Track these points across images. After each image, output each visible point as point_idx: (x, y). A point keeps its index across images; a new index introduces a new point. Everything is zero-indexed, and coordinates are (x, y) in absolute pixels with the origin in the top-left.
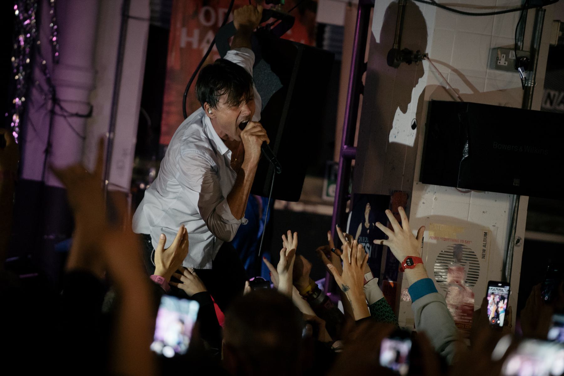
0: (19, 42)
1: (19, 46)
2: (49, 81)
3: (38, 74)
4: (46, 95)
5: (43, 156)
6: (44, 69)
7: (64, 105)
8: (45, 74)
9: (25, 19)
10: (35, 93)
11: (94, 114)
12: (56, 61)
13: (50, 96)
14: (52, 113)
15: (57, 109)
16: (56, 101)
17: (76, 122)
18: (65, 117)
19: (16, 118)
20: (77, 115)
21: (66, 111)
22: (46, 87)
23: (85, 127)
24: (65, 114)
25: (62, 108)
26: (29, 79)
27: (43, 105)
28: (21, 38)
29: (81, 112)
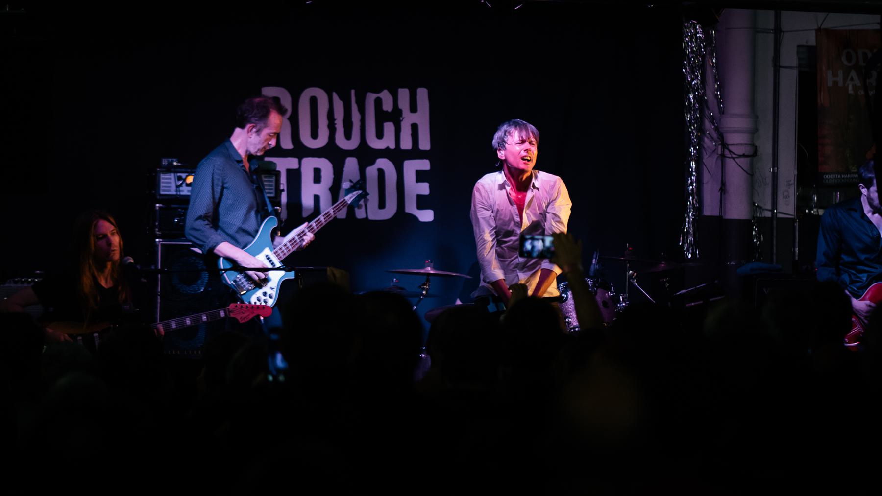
0: (690, 99)
1: (690, 103)
2: (717, 129)
3: (707, 123)
4: (716, 142)
5: (719, 194)
6: (712, 120)
7: (731, 148)
8: (714, 124)
9: (693, 80)
10: (707, 140)
11: (758, 153)
12: (722, 112)
13: (720, 143)
14: (723, 156)
15: (727, 152)
16: (725, 146)
17: (743, 161)
18: (733, 158)
19: (693, 164)
20: (744, 156)
21: (735, 154)
22: (715, 135)
23: (752, 165)
24: (734, 156)
25: (730, 151)
26: (701, 130)
27: (714, 151)
28: (691, 96)
29: (746, 154)
